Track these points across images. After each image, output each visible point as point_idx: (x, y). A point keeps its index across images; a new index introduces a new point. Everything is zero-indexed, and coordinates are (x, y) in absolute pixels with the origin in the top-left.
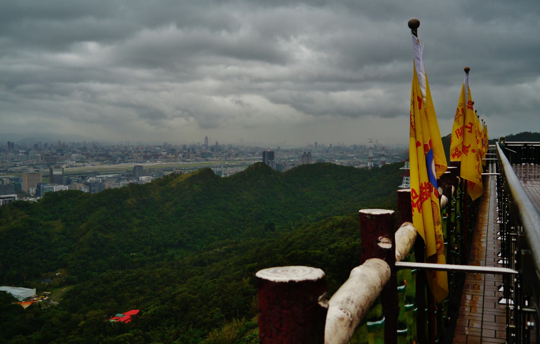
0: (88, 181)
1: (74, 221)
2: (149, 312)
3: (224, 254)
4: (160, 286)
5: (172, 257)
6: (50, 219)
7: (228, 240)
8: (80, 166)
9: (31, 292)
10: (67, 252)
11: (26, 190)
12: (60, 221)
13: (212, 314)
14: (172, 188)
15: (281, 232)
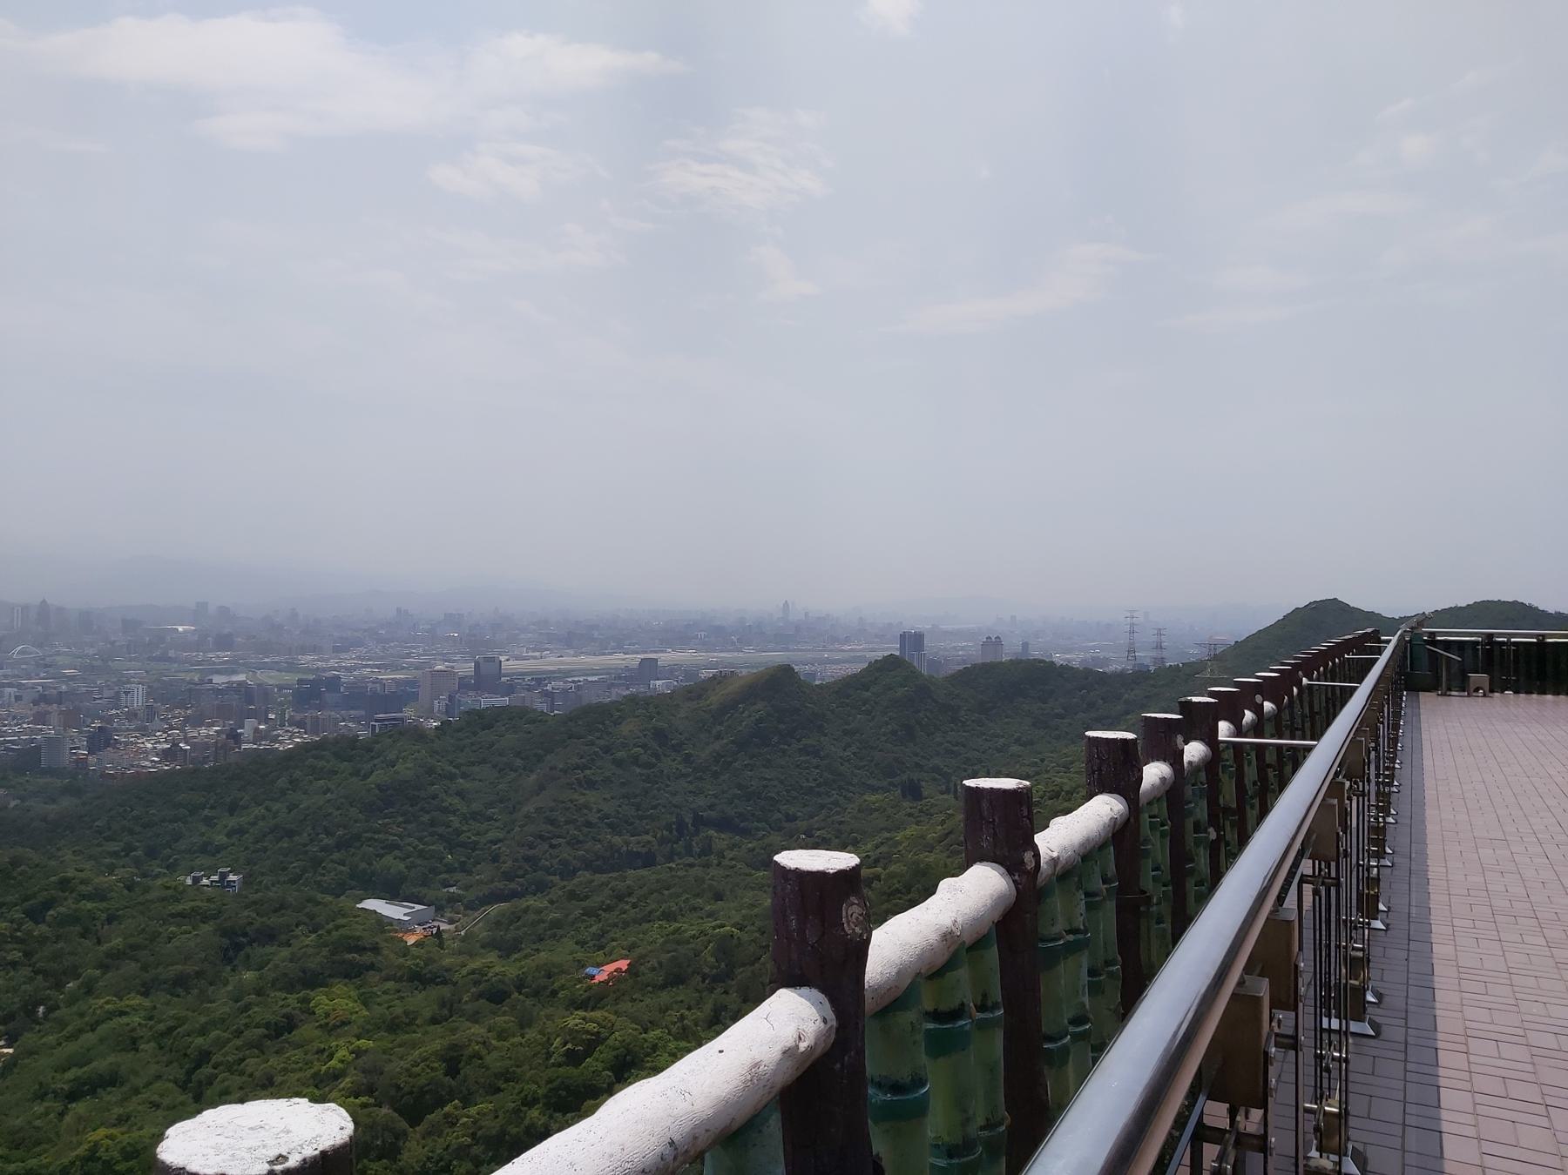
0: (549, 688)
8: (535, 658)
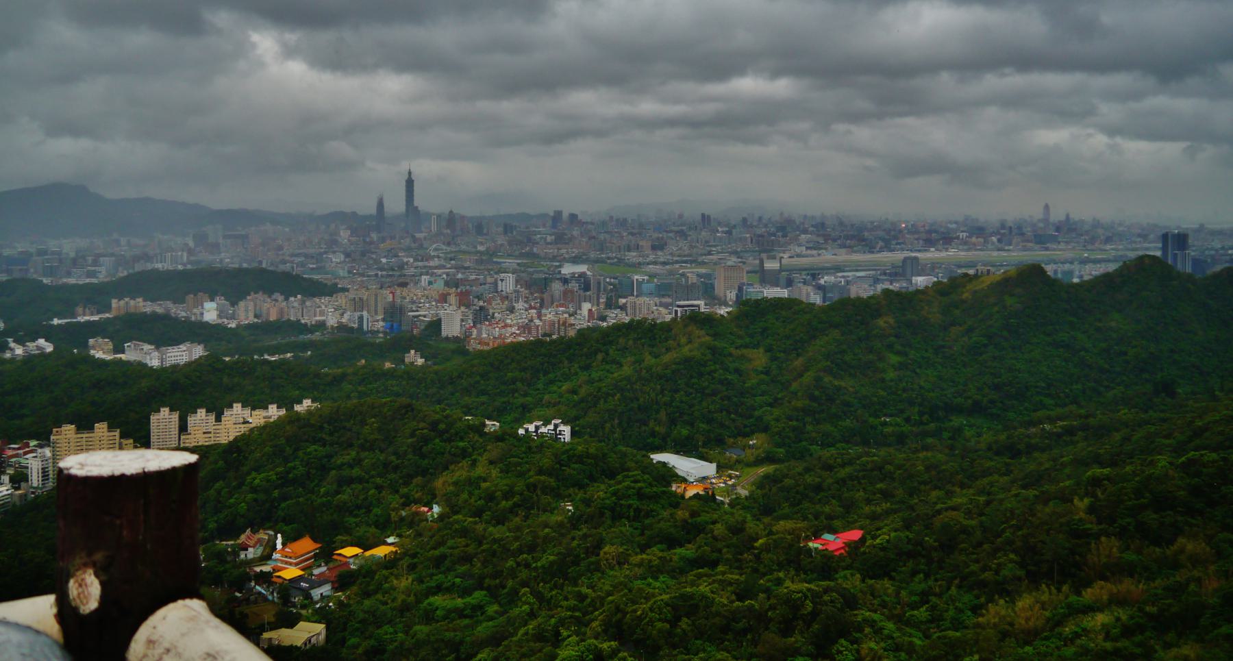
1: (784, 352)
2: (878, 541)
3: (1059, 436)
4: (922, 487)
5: (958, 431)
6: (746, 347)
7: (1073, 407)
9: (709, 469)
10: (771, 405)
11: (722, 295)
12: (761, 350)
13: (999, 565)
14: (964, 302)
15: (1191, 402)
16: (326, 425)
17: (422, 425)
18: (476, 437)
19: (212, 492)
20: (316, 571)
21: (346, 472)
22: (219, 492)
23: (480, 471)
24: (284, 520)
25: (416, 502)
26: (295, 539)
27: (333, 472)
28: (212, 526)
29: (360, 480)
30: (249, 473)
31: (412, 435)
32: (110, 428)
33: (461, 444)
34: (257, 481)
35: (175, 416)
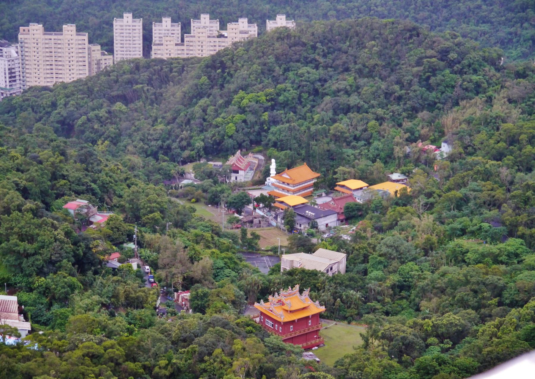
16: (319, 45)
17: (430, 52)
18: (493, 71)
19: (197, 108)
20: (320, 201)
21: (343, 99)
22: (204, 111)
23: (499, 108)
24: (275, 145)
25: (424, 138)
26: (289, 167)
27: (328, 98)
28: (199, 144)
29: (359, 109)
30: (236, 92)
31: (419, 63)
32: (79, 30)
33: (475, 78)
34: (245, 101)
35: (139, 24)
